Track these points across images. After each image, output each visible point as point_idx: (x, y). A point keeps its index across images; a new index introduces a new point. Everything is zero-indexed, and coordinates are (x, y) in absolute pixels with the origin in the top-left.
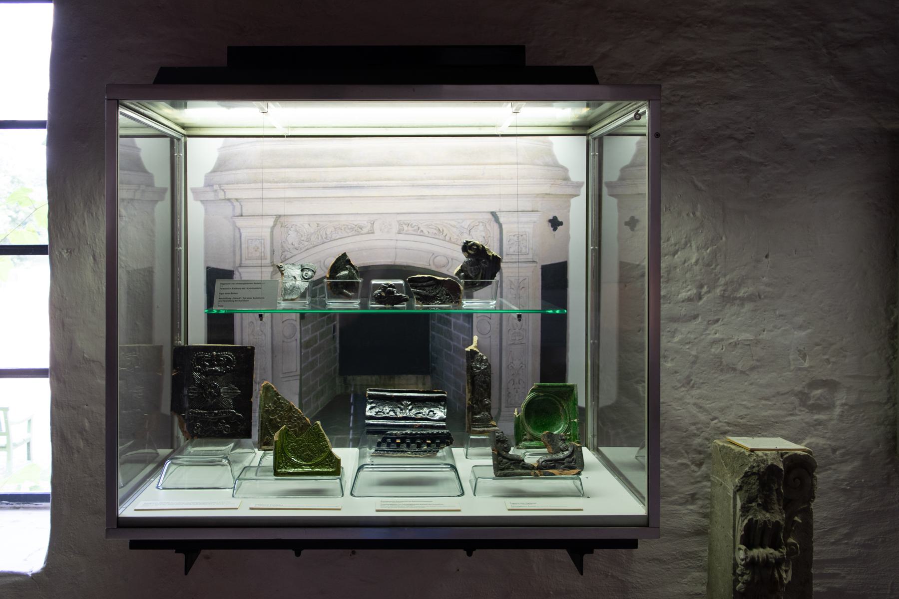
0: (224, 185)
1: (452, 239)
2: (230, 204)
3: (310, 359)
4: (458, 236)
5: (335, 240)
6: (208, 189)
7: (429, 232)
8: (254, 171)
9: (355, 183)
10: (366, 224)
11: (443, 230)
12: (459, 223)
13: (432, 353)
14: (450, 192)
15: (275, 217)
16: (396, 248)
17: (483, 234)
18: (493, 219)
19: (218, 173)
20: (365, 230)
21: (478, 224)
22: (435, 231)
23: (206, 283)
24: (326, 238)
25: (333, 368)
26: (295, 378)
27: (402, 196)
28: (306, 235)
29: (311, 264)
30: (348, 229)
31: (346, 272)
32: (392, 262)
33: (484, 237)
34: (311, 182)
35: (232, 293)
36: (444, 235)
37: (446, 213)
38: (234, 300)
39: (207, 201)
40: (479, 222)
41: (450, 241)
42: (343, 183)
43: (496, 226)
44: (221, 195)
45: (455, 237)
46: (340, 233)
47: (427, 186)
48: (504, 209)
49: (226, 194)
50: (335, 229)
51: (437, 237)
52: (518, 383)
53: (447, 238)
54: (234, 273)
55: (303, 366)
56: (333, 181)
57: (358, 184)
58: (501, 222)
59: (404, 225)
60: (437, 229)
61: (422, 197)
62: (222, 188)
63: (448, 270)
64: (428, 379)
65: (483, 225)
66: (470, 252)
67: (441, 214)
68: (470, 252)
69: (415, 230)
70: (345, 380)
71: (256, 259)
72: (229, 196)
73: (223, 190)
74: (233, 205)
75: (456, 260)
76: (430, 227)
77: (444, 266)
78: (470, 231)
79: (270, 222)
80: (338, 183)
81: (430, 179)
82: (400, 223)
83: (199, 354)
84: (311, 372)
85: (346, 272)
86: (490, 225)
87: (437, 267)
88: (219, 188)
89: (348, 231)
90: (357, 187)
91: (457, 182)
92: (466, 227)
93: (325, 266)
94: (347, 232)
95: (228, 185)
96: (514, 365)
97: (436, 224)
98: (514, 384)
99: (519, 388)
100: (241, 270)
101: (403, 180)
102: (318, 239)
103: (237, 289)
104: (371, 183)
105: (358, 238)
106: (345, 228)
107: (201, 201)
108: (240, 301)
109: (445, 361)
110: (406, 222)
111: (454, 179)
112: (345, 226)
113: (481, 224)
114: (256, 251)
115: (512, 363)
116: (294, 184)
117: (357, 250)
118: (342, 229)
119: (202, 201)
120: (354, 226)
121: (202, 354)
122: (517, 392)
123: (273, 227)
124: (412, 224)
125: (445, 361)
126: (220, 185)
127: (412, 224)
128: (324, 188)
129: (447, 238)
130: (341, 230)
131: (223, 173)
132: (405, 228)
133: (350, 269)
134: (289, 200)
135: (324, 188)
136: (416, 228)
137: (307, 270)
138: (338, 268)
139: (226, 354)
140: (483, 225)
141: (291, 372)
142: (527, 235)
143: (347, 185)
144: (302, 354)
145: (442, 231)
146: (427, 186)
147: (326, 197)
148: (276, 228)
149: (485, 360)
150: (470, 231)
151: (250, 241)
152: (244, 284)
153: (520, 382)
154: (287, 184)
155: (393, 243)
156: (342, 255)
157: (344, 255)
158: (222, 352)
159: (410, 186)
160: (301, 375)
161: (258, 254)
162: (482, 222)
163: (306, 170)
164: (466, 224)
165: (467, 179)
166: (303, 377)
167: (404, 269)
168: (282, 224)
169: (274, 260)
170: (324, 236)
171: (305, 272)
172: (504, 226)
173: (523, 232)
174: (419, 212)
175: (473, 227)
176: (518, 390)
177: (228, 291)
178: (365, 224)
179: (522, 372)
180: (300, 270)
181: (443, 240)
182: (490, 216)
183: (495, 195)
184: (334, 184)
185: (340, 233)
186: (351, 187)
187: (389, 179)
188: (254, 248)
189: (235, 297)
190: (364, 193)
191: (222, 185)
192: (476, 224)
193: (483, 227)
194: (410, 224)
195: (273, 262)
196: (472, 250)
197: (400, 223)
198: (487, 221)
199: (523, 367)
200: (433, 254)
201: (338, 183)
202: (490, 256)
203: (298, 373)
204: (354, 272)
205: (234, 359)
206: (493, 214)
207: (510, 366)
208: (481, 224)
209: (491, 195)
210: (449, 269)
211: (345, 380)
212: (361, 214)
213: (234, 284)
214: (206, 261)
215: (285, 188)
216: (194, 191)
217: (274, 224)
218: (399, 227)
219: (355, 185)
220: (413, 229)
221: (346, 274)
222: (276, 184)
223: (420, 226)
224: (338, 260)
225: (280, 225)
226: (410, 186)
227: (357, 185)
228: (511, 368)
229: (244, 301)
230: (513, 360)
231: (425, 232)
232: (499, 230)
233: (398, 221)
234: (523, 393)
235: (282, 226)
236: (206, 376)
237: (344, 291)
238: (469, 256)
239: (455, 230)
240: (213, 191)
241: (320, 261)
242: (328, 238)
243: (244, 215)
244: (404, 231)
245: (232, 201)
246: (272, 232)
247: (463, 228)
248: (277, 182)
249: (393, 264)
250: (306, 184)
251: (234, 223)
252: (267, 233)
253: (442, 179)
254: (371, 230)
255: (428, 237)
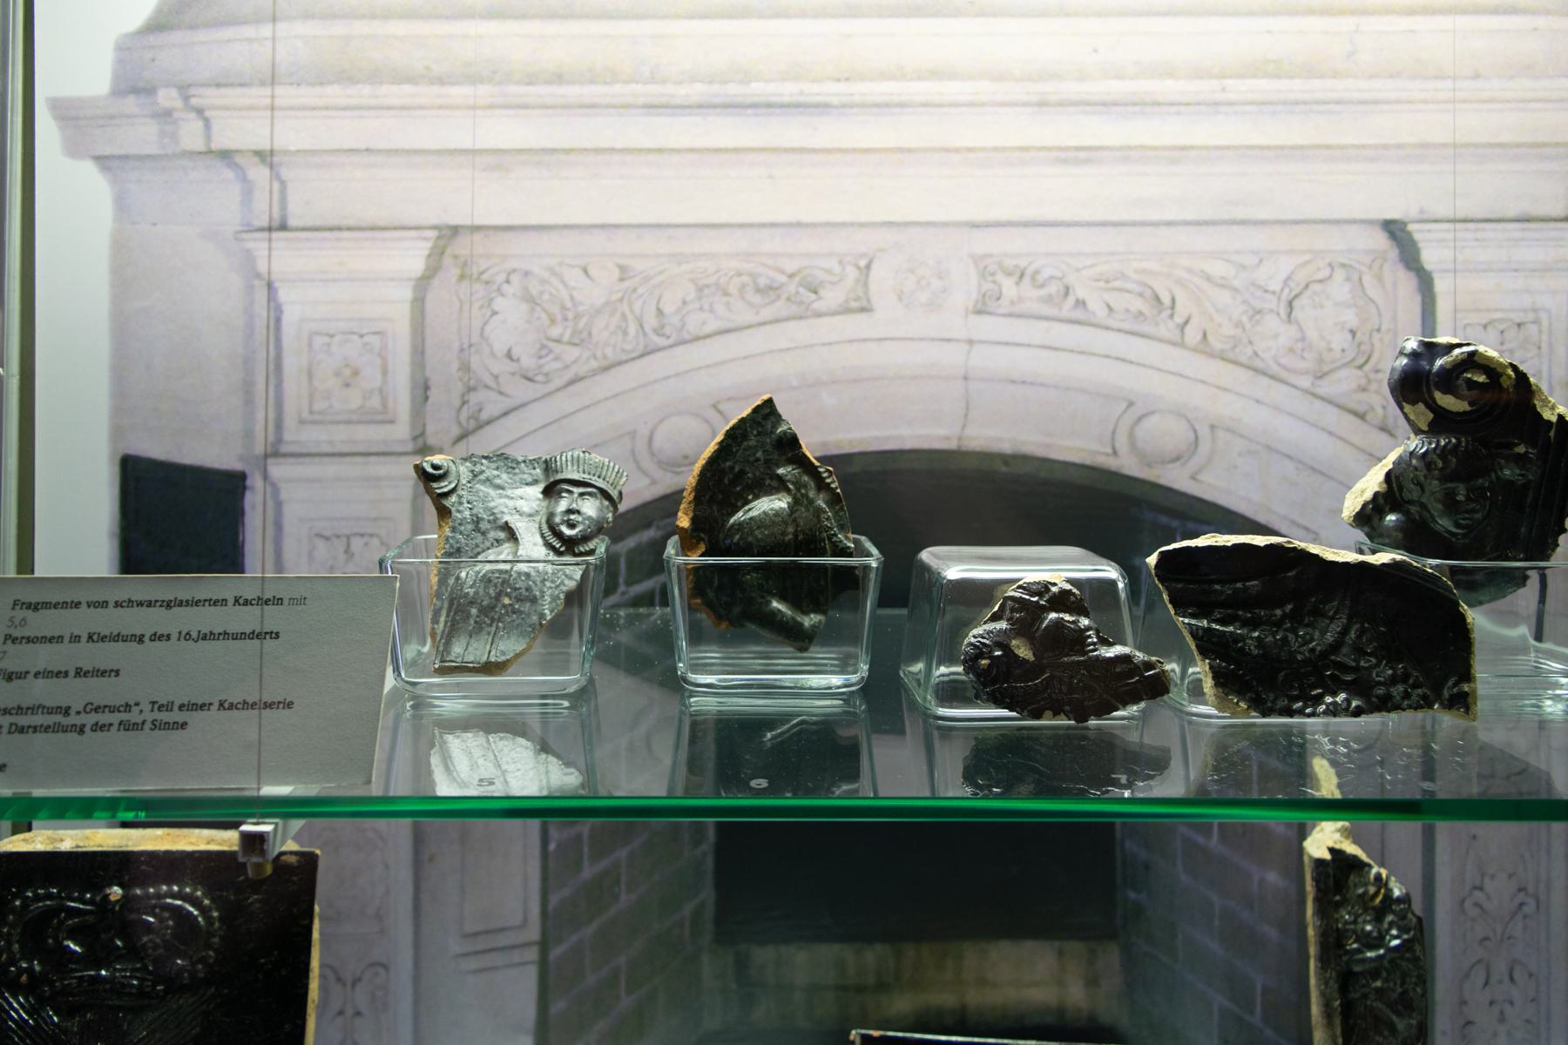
0: (201, 91)
1: (1210, 338)
2: (229, 174)
3: (588, 872)
4: (1239, 324)
5: (698, 338)
6: (131, 104)
7: (1110, 309)
8: (339, 28)
9: (788, 91)
10: (837, 269)
11: (1173, 300)
12: (1243, 267)
13: (1128, 844)
14: (1203, 132)
15: (433, 234)
16: (966, 378)
17: (1350, 318)
18: (1394, 253)
19: (176, 37)
20: (832, 297)
21: (1327, 272)
22: (1137, 304)
23: (117, 530)
24: (659, 331)
25: (688, 909)
26: (516, 956)
27: (996, 149)
28: (570, 315)
29: (596, 458)
30: (758, 290)
31: (776, 503)
32: (947, 438)
33: (1353, 333)
34: (592, 82)
35: (79, 673)
36: (1179, 320)
37: (1187, 223)
38: (92, 718)
39: (125, 158)
40: (1330, 265)
41: (1204, 347)
42: (733, 90)
43: (1407, 284)
44: (191, 135)
45: (1228, 330)
46: (720, 309)
47: (1106, 105)
48: (1443, 210)
49: (215, 128)
50: (700, 290)
51: (1146, 328)
52: (1506, 979)
53: (1192, 335)
54: (248, 482)
55: (554, 900)
56: (693, 79)
57: (801, 93)
58: (1427, 267)
59: (1000, 277)
60: (1148, 293)
61: (1082, 155)
62: (194, 101)
63: (1193, 478)
64: (1111, 956)
65: (1348, 279)
66: (1447, 401)
67: (1164, 231)
68: (1447, 401)
69: (1049, 299)
70: (742, 965)
71: (348, 422)
72: (224, 138)
73: (200, 111)
74: (244, 179)
75: (1228, 430)
76: (1117, 284)
77: (1178, 459)
78: (1290, 303)
79: (411, 258)
80: (716, 88)
81: (1119, 77)
82: (985, 268)
83: (37, 898)
84: (591, 929)
85: (776, 503)
86: (1380, 279)
87: (1146, 460)
88: (179, 104)
89: (757, 299)
90: (798, 105)
91: (1239, 88)
92: (1275, 286)
93: (652, 454)
94: (750, 304)
95: (224, 91)
96: (1489, 898)
97: (1143, 271)
98: (1486, 984)
99: (1512, 1003)
100: (277, 470)
101: (999, 77)
102: (625, 333)
103: (117, 638)
104: (860, 90)
105: (799, 332)
106: (743, 286)
107: (99, 159)
108: (126, 726)
109: (1184, 878)
110: (1009, 263)
111: (1222, 76)
112: (745, 279)
113: (1339, 275)
114: (347, 385)
115: (1481, 889)
116: (516, 91)
117: (794, 383)
118: (733, 290)
119: (102, 161)
120: (783, 279)
121: (49, 896)
122: (1502, 1018)
123: (422, 284)
124: (1037, 272)
125: (1184, 878)
126: (185, 90)
127: (1037, 272)
128: (652, 107)
129: (1192, 335)
130: (726, 294)
131: (201, 36)
132: (1009, 287)
133: (799, 485)
134: (499, 160)
135: (652, 107)
136: (1053, 288)
137: (577, 490)
138: (733, 482)
139: (174, 896)
140: (1348, 279)
141: (502, 930)
142: (1545, 323)
143: (756, 99)
144: (552, 847)
145: (1166, 300)
146: (1106, 105)
147: (660, 151)
148: (436, 282)
149: (1399, 900)
150: (1290, 303)
151: (319, 341)
152: (168, 605)
153: (1517, 975)
154: (483, 90)
155: (952, 357)
156: (756, 410)
157: (766, 412)
158: (155, 884)
159: (1026, 104)
160: (544, 945)
161: (354, 400)
162: (1343, 265)
163: (574, 27)
164: (1274, 274)
165: (1278, 77)
166: (556, 952)
167: (1004, 469)
168: (465, 264)
169: (430, 429)
170: (651, 321)
171: (563, 505)
172: (1441, 286)
173: (1525, 311)
174: (1066, 217)
175: (1307, 286)
176: (1507, 1008)
177: (43, 657)
178: (828, 271)
179: (1525, 928)
180: (536, 492)
181: (1174, 344)
182: (1380, 241)
183: (1399, 146)
184: (697, 91)
185: (720, 309)
186: (769, 106)
187: (936, 74)
188: (337, 374)
189: (99, 701)
190: (827, 132)
191: (193, 91)
192: (1320, 276)
193: (1346, 288)
194: (1029, 272)
195: (423, 434)
196: (1457, 396)
197: (985, 268)
198: (1367, 260)
199: (1530, 908)
200: (1131, 404)
201: (716, 88)
202: (1549, 422)
203: (534, 933)
204: (821, 503)
205: (209, 919)
206: (1395, 230)
207: (1468, 904)
208: (1339, 275)
209: (1386, 147)
210: (1200, 470)
211: (742, 965)
212: (814, 225)
213: (105, 604)
214: (117, 432)
215: (474, 108)
216: (68, 113)
217: (428, 268)
218: (980, 286)
219: (786, 99)
220: (1043, 292)
221: (777, 513)
222: (436, 89)
223: (1071, 279)
224: (736, 435)
225: (455, 272)
226: (1026, 104)
227: (802, 99)
228: (1474, 912)
229: (156, 725)
230: (1483, 875)
231: (1096, 306)
232: (1418, 299)
233: (976, 259)
234: (1528, 1021)
235: (462, 277)
236: (67, 1012)
237: (775, 604)
238: (1441, 422)
239: (1224, 297)
240: (155, 115)
241: (633, 434)
242: (667, 330)
243: (292, 222)
244: (1004, 302)
245: (238, 159)
246: (419, 302)
247: (1259, 293)
248: (441, 81)
249: (952, 445)
250: (573, 92)
251: (249, 257)
252: (394, 306)
253: (1171, 73)
254: (857, 299)
255: (1107, 328)
